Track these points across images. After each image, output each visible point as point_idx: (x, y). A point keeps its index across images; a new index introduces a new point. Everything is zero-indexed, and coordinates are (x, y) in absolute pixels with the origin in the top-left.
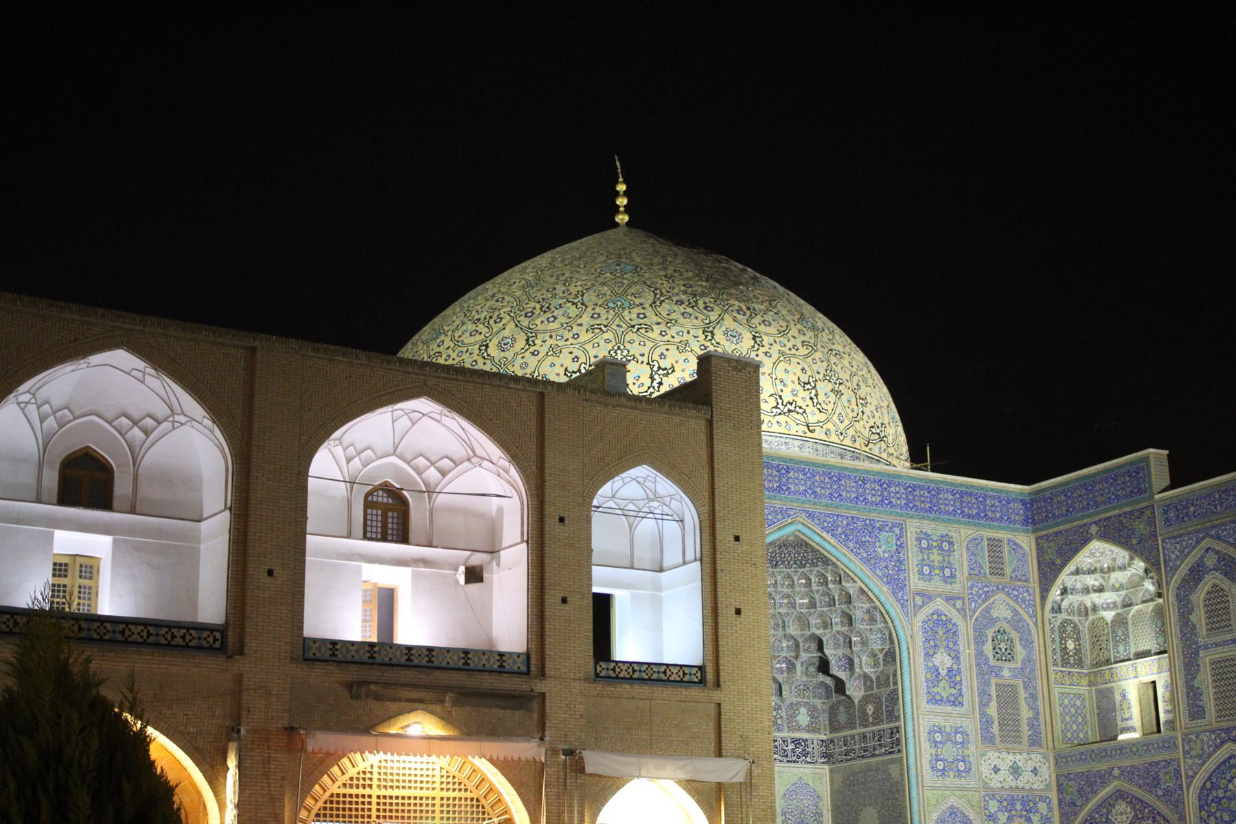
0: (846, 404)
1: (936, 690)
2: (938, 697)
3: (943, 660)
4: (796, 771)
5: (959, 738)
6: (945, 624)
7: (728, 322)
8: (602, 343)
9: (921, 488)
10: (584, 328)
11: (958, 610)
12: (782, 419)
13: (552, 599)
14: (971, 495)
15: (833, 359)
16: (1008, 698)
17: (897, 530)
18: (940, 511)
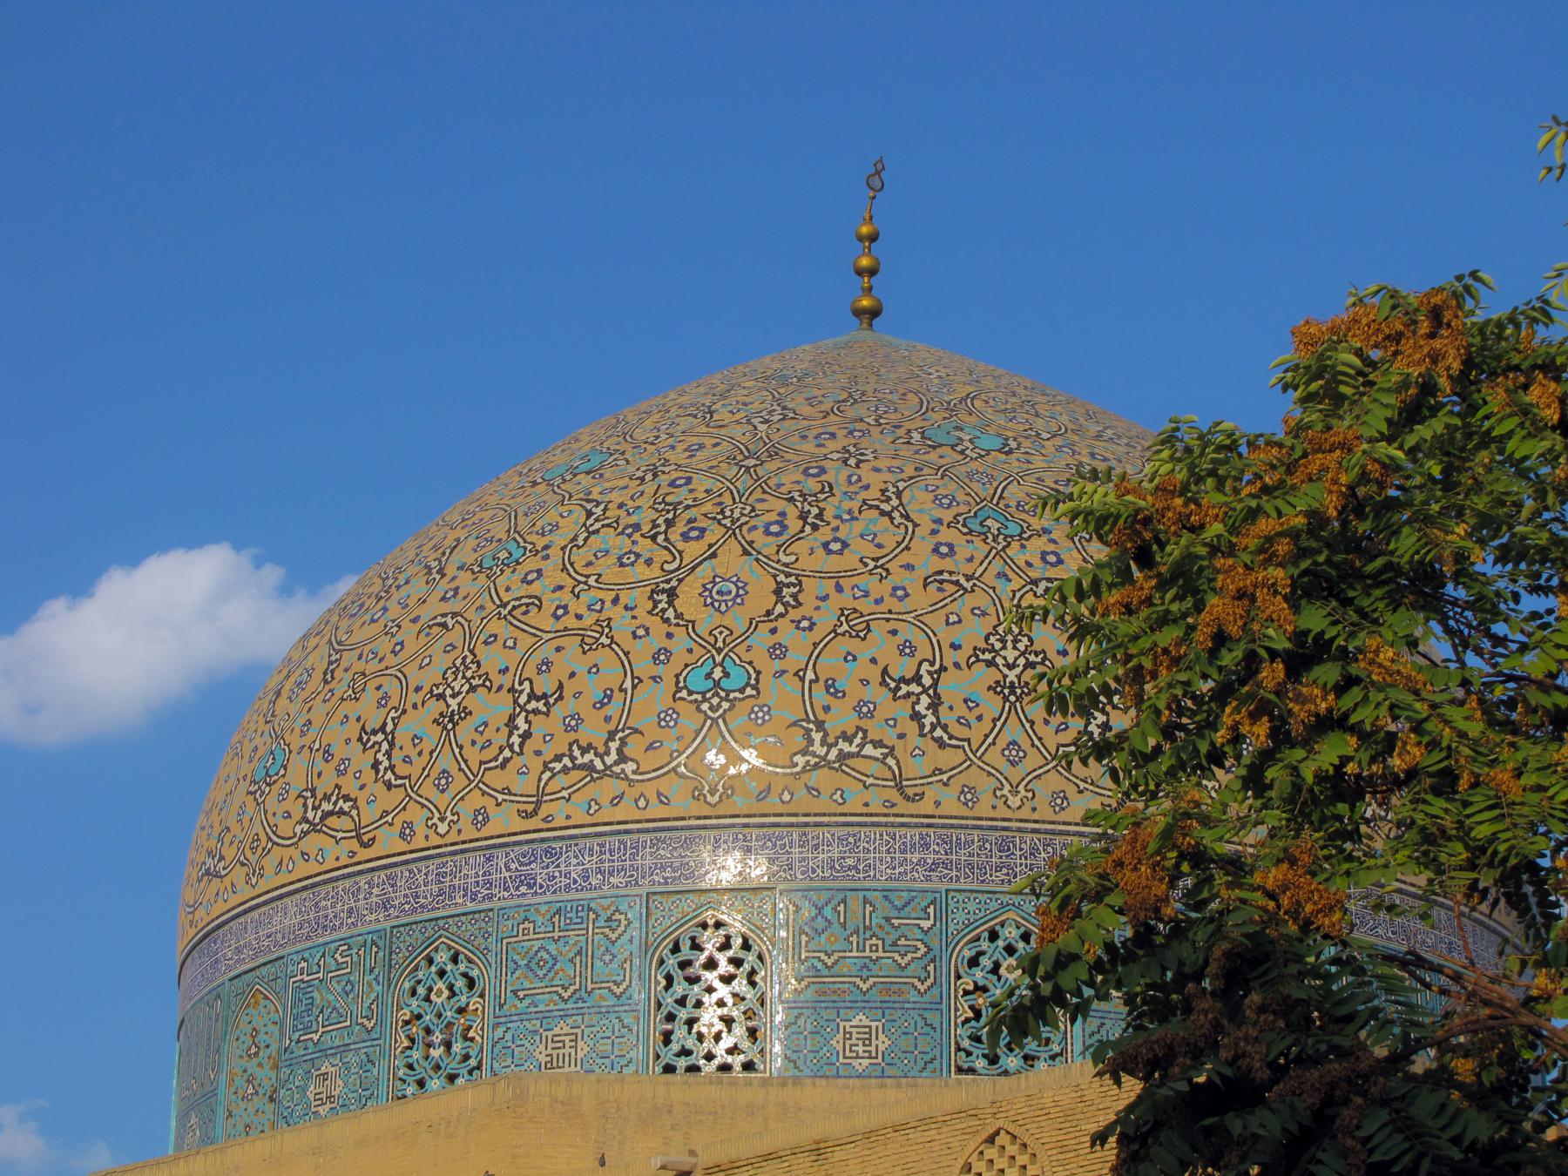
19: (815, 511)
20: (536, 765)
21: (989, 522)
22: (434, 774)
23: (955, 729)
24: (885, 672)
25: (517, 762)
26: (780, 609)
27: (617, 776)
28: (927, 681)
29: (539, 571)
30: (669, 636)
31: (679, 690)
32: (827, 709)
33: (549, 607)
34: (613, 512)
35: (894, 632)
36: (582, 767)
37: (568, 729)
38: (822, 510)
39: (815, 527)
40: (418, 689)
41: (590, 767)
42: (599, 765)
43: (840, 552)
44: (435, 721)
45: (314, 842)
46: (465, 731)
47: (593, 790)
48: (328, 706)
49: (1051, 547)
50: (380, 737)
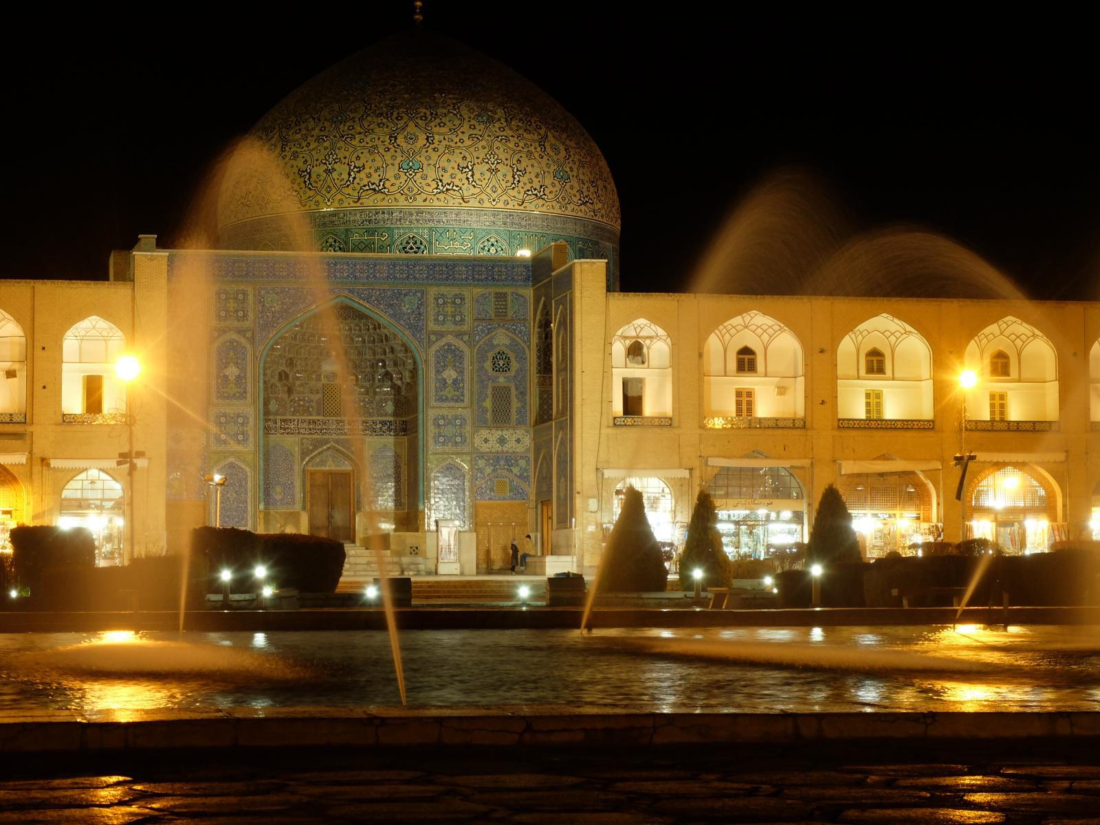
0: (501, 178)
1: (442, 393)
2: (444, 398)
3: (450, 374)
4: (383, 440)
5: (458, 422)
6: (453, 352)
7: (411, 128)
8: (322, 150)
10: (314, 139)
11: (465, 342)
12: (442, 196)
13: (38, 386)
14: (482, 266)
15: (497, 144)
16: (501, 396)
17: (419, 295)
20: (358, 187)
21: (484, 118)
23: (478, 182)
26: (428, 144)
27: (382, 193)
28: (470, 168)
29: (353, 126)
30: (396, 151)
31: (400, 168)
32: (442, 176)
33: (358, 139)
35: (461, 153)
36: (372, 189)
38: (437, 112)
39: (435, 118)
40: (317, 160)
41: (374, 190)
42: (377, 189)
43: (444, 126)
44: (324, 171)
46: (335, 175)
49: (501, 125)
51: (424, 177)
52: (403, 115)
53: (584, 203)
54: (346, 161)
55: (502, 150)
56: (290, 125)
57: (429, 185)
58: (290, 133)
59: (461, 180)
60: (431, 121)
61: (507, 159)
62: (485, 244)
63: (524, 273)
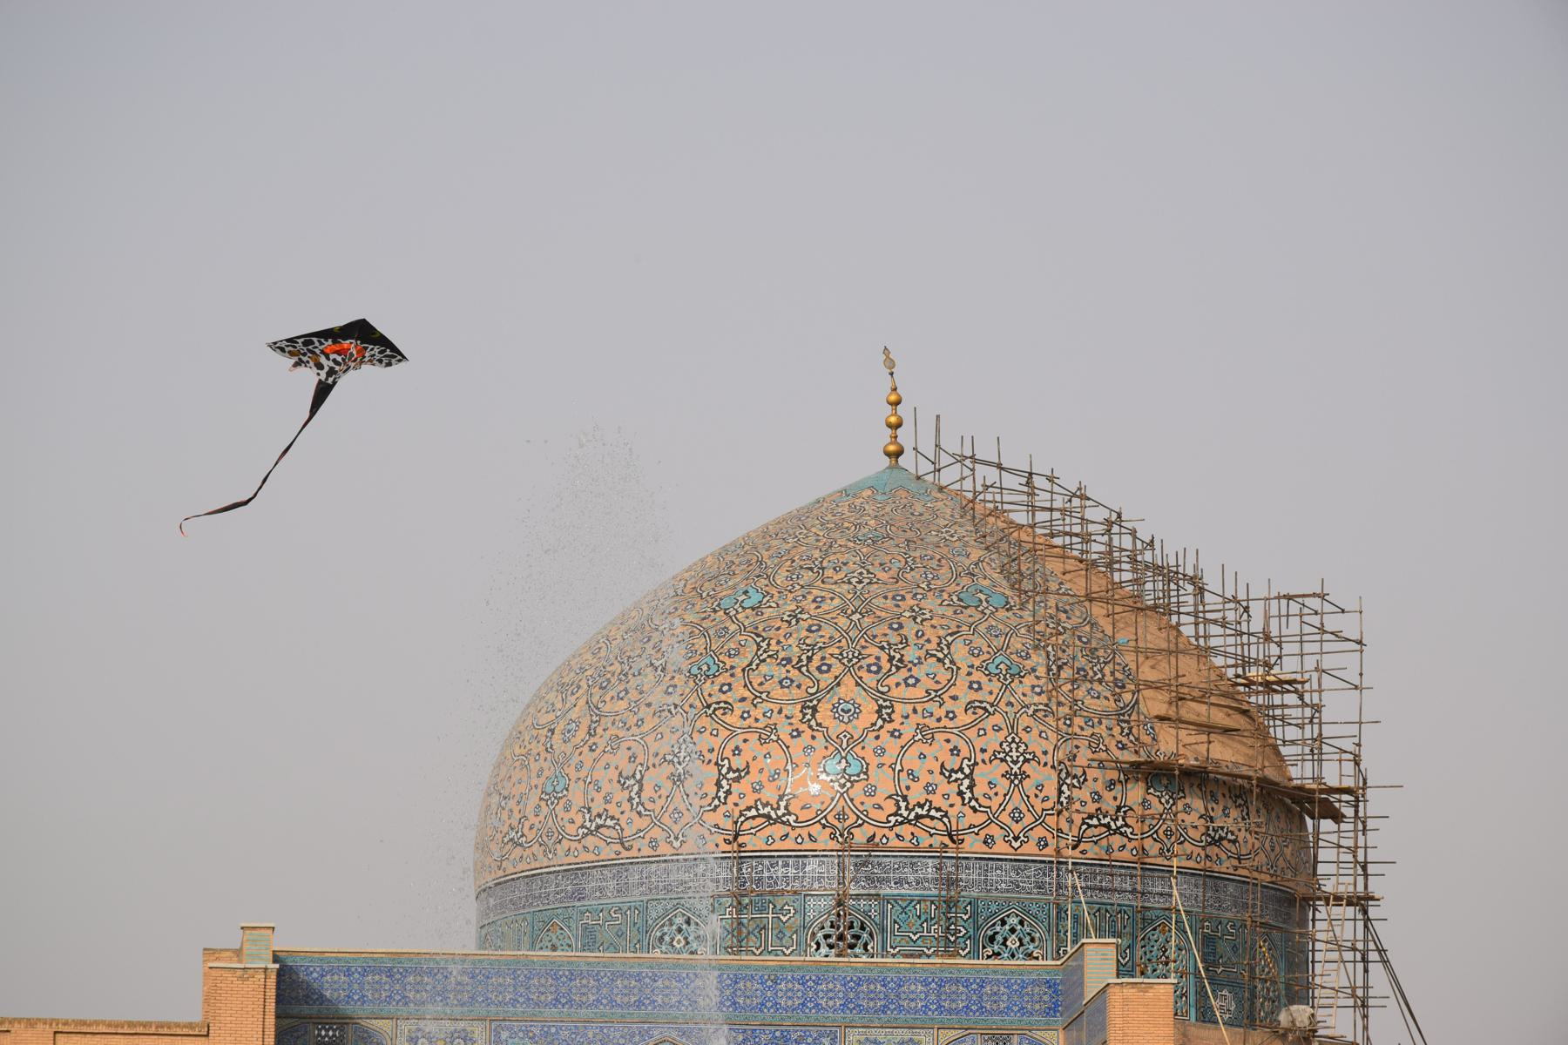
0: (1032, 792)
7: (848, 689)
9: (869, 981)
12: (906, 830)
15: (1025, 721)
18: (900, 1008)
19: (898, 656)
22: (671, 810)
23: (983, 801)
24: (942, 766)
25: (723, 809)
26: (880, 722)
28: (967, 771)
30: (813, 737)
32: (908, 788)
33: (738, 712)
34: (774, 647)
35: (948, 741)
36: (763, 816)
37: (755, 791)
39: (898, 668)
41: (768, 817)
43: (914, 685)
45: (590, 841)
46: (690, 785)
47: (769, 831)
48: (595, 755)
49: (1036, 682)
50: (632, 782)
51: (871, 792)
52: (833, 661)
53: (1216, 842)
54: (713, 757)
55: (1035, 732)
56: (609, 681)
57: (880, 807)
58: (608, 699)
59: (946, 796)
60: (888, 674)
61: (1045, 753)
62: (998, 928)
63: (1046, 998)
